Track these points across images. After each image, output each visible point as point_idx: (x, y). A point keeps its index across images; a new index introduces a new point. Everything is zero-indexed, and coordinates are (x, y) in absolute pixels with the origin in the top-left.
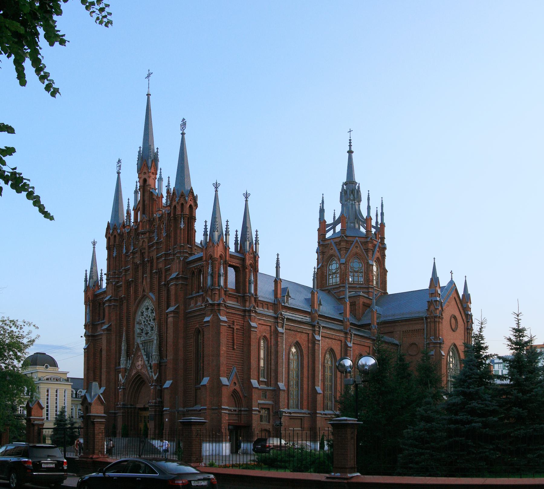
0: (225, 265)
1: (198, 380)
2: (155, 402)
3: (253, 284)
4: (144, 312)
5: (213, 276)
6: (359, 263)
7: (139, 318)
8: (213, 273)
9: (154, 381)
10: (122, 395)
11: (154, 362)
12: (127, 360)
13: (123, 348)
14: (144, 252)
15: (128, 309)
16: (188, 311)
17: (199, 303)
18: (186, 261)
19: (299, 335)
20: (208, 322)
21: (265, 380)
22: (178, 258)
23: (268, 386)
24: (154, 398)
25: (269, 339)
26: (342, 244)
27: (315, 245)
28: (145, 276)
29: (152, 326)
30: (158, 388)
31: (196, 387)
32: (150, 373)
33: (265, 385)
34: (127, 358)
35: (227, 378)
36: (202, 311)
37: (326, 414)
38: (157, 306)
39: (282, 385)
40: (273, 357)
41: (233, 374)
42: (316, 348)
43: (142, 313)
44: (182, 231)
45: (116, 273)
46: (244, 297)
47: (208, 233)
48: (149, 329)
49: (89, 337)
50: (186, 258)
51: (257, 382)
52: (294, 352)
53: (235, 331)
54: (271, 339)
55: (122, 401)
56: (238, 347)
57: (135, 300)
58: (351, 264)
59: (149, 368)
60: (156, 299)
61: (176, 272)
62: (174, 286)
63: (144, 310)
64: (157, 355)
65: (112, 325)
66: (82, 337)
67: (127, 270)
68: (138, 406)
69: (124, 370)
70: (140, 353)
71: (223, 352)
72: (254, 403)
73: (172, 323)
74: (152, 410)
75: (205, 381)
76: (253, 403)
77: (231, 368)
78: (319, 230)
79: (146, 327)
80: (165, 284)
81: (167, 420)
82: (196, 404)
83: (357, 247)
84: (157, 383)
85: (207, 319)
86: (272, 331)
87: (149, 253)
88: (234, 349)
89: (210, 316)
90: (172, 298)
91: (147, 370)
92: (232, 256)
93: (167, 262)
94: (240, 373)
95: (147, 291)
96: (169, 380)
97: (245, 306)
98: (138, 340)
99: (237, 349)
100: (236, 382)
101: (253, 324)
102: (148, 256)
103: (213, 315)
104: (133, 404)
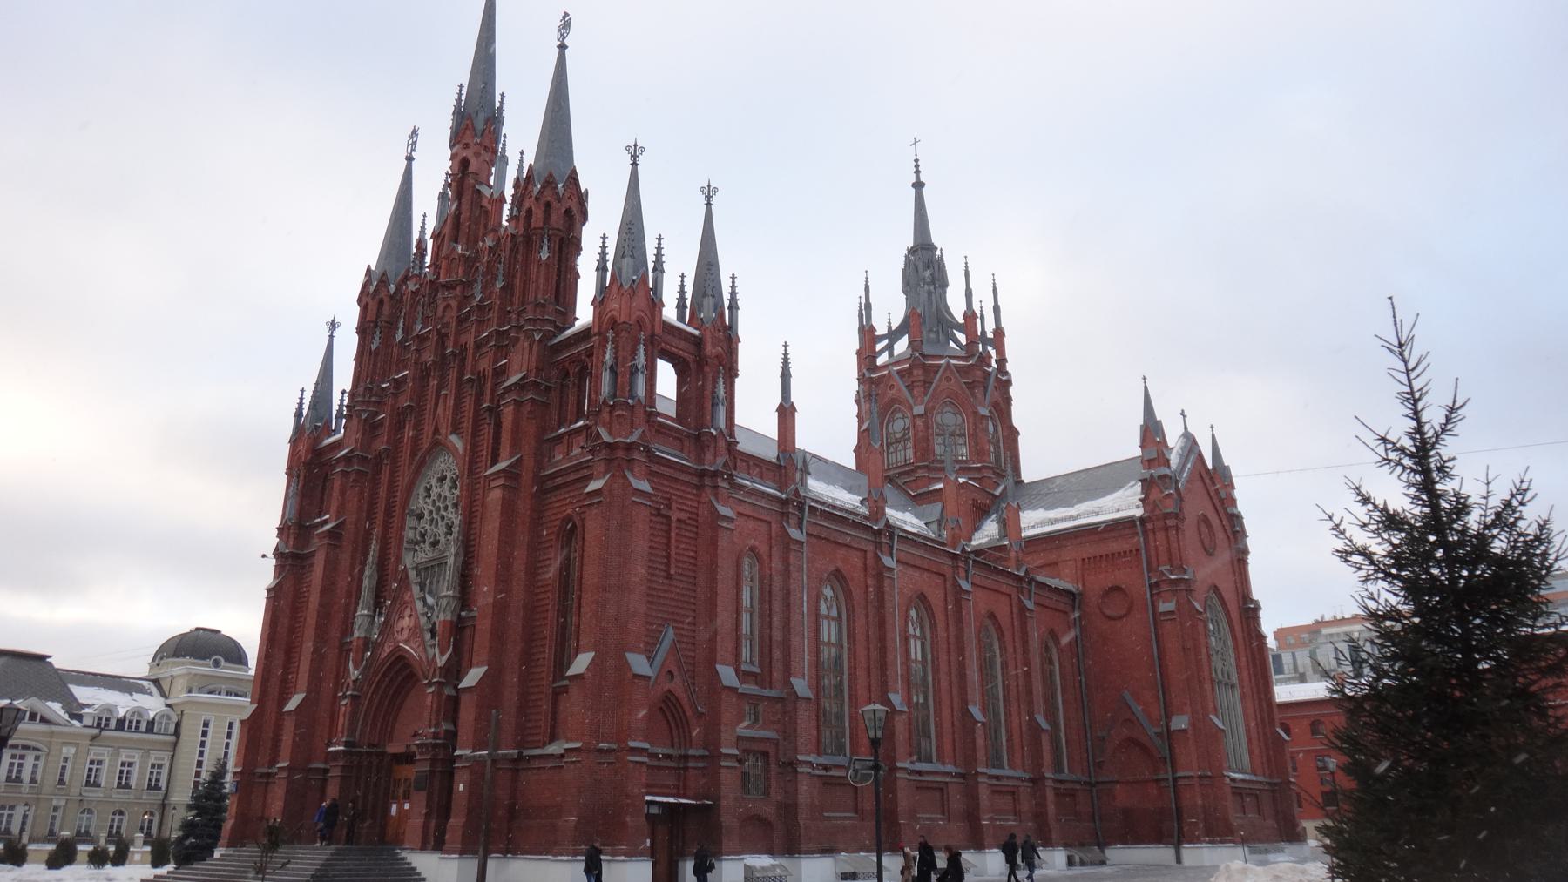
0: (650, 347)
1: (562, 663)
2: (434, 733)
3: (723, 404)
4: (434, 488)
5: (616, 373)
6: (954, 413)
7: (419, 503)
8: (617, 364)
9: (438, 672)
10: (347, 715)
11: (443, 617)
12: (374, 618)
13: (366, 582)
14: (447, 335)
15: (392, 483)
16: (547, 473)
17: (576, 451)
18: (549, 344)
19: (842, 552)
20: (597, 492)
21: (756, 670)
22: (529, 334)
23: (762, 687)
24: (433, 722)
25: (765, 558)
26: (915, 372)
27: (850, 384)
28: (443, 392)
29: (449, 522)
30: (448, 691)
31: (554, 685)
32: (431, 651)
33: (756, 684)
34: (375, 612)
35: (648, 658)
36: (581, 472)
37: (919, 773)
38: (466, 467)
39: (801, 686)
40: (777, 606)
41: (664, 645)
42: (887, 589)
43: (428, 490)
44: (542, 269)
45: (374, 392)
46: (698, 438)
47: (609, 265)
48: (442, 529)
49: (286, 558)
50: (549, 336)
51: (734, 673)
52: (829, 598)
53: (674, 525)
54: (770, 556)
55: (345, 734)
56: (680, 571)
57: (413, 454)
58: (938, 418)
59: (428, 636)
60: (465, 452)
61: (522, 372)
62: (512, 407)
63: (434, 482)
64: (454, 597)
65: (347, 521)
66: (264, 556)
67: (398, 384)
68: (394, 748)
69: (361, 642)
70: (409, 594)
71: (637, 580)
72: (726, 736)
73: (500, 503)
74: (423, 757)
75: (581, 663)
76: (722, 734)
77: (660, 629)
78: (859, 353)
79: (433, 527)
80: (489, 409)
81: (461, 787)
82: (553, 738)
83: (948, 379)
84: (444, 677)
85: (594, 486)
86: (773, 535)
87: (458, 333)
88: (669, 577)
89: (604, 477)
90: (506, 437)
91: (423, 641)
92: (667, 327)
93: (503, 350)
94: (684, 646)
95: (443, 431)
96: (479, 665)
97: (700, 461)
98: (409, 560)
99: (679, 578)
100: (673, 670)
101: (724, 510)
102: (455, 344)
103: (613, 475)
104: (376, 742)
